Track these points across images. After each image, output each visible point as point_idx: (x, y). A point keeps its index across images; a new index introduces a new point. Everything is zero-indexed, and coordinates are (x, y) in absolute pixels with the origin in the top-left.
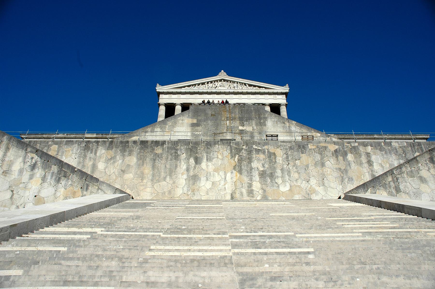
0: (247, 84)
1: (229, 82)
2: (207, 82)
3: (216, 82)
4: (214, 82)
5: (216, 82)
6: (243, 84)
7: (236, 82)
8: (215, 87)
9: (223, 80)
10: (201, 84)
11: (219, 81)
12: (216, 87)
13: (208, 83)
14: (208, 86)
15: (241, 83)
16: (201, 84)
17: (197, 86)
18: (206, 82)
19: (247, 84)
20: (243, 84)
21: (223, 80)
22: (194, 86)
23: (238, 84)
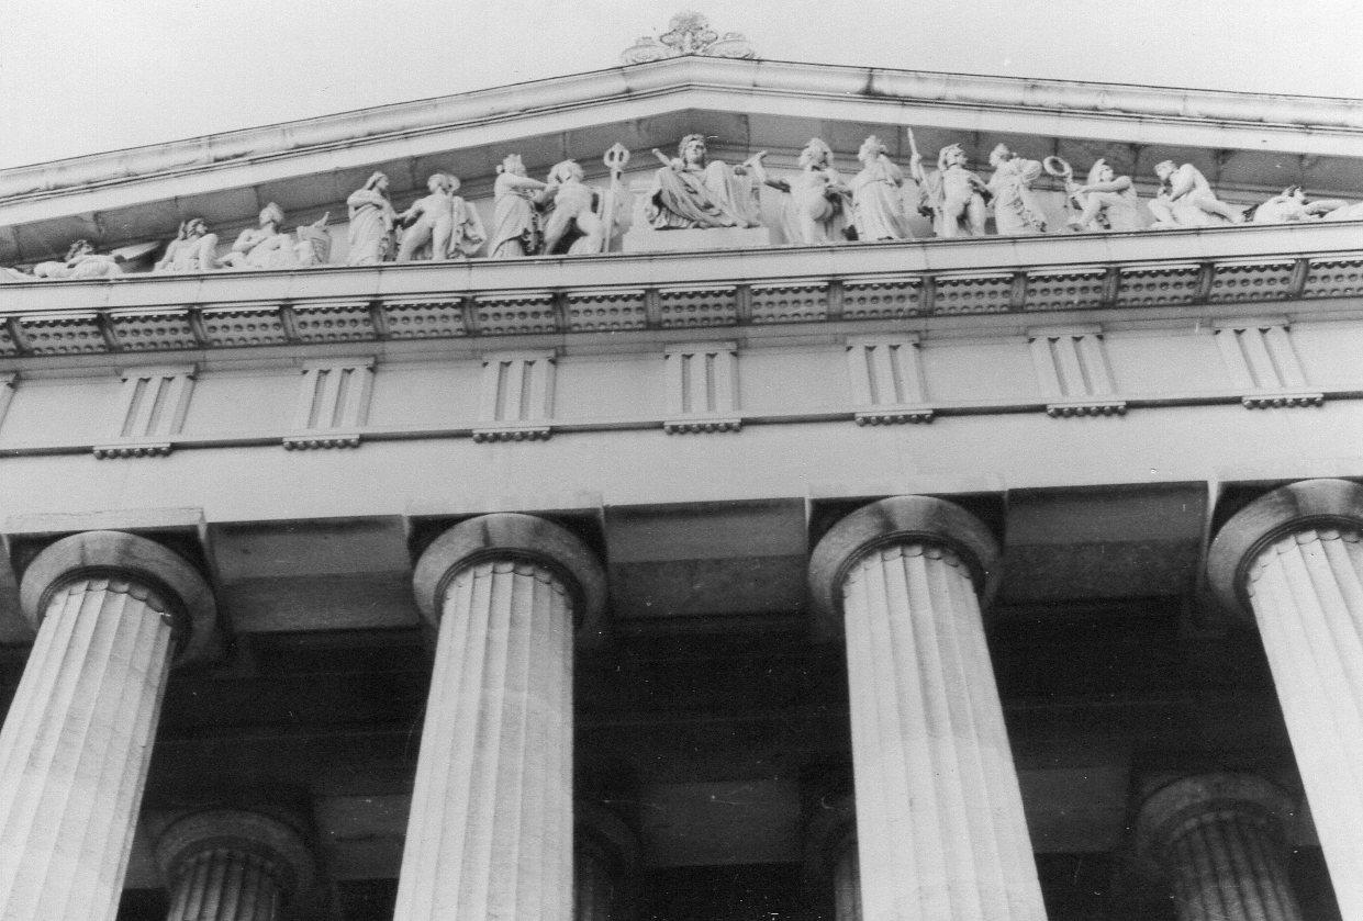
0: (1181, 155)
1: (816, 146)
2: (381, 167)
3: (566, 169)
4: (538, 170)
5: (566, 169)
6: (1100, 172)
7: (951, 153)
8: (553, 228)
9: (690, 147)
10: (270, 213)
11: (617, 148)
12: (572, 233)
13: (407, 184)
14: (409, 237)
15: (1056, 145)
16: (270, 213)
17: (190, 251)
18: (369, 170)
19: (1164, 169)
20: (1100, 172)
21: (690, 147)
22: (130, 252)
23: (1004, 167)
